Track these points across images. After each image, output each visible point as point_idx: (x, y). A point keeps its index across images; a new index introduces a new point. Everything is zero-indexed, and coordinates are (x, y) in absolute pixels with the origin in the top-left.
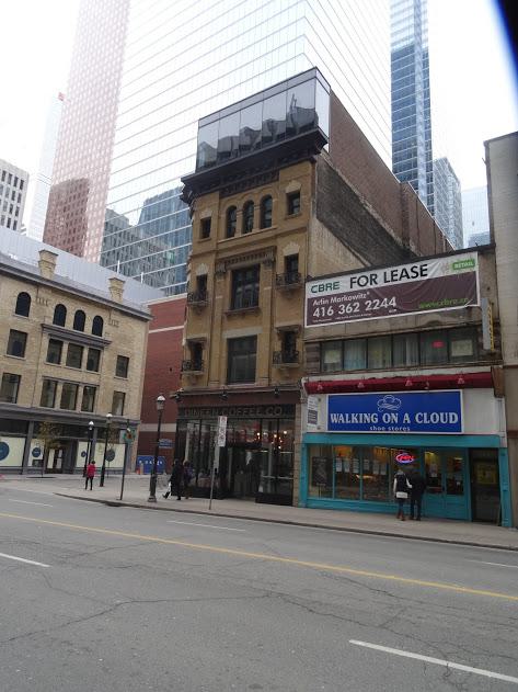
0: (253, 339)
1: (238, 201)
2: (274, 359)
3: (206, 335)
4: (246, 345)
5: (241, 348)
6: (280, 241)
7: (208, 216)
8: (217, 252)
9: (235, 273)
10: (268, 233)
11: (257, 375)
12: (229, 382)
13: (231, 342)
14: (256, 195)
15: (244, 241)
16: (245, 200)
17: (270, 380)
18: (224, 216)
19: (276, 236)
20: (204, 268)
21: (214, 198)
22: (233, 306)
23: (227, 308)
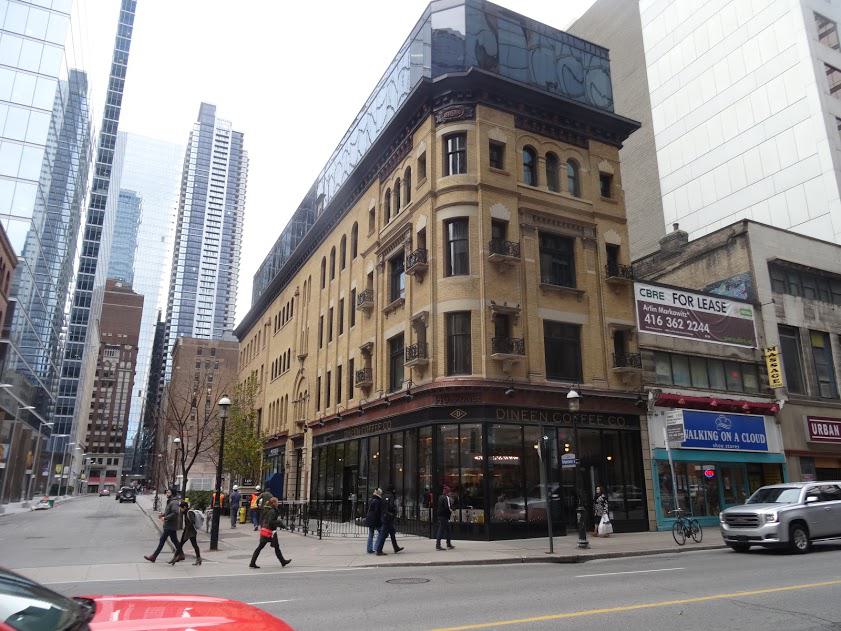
3: (373, 340)
15: (400, 219)
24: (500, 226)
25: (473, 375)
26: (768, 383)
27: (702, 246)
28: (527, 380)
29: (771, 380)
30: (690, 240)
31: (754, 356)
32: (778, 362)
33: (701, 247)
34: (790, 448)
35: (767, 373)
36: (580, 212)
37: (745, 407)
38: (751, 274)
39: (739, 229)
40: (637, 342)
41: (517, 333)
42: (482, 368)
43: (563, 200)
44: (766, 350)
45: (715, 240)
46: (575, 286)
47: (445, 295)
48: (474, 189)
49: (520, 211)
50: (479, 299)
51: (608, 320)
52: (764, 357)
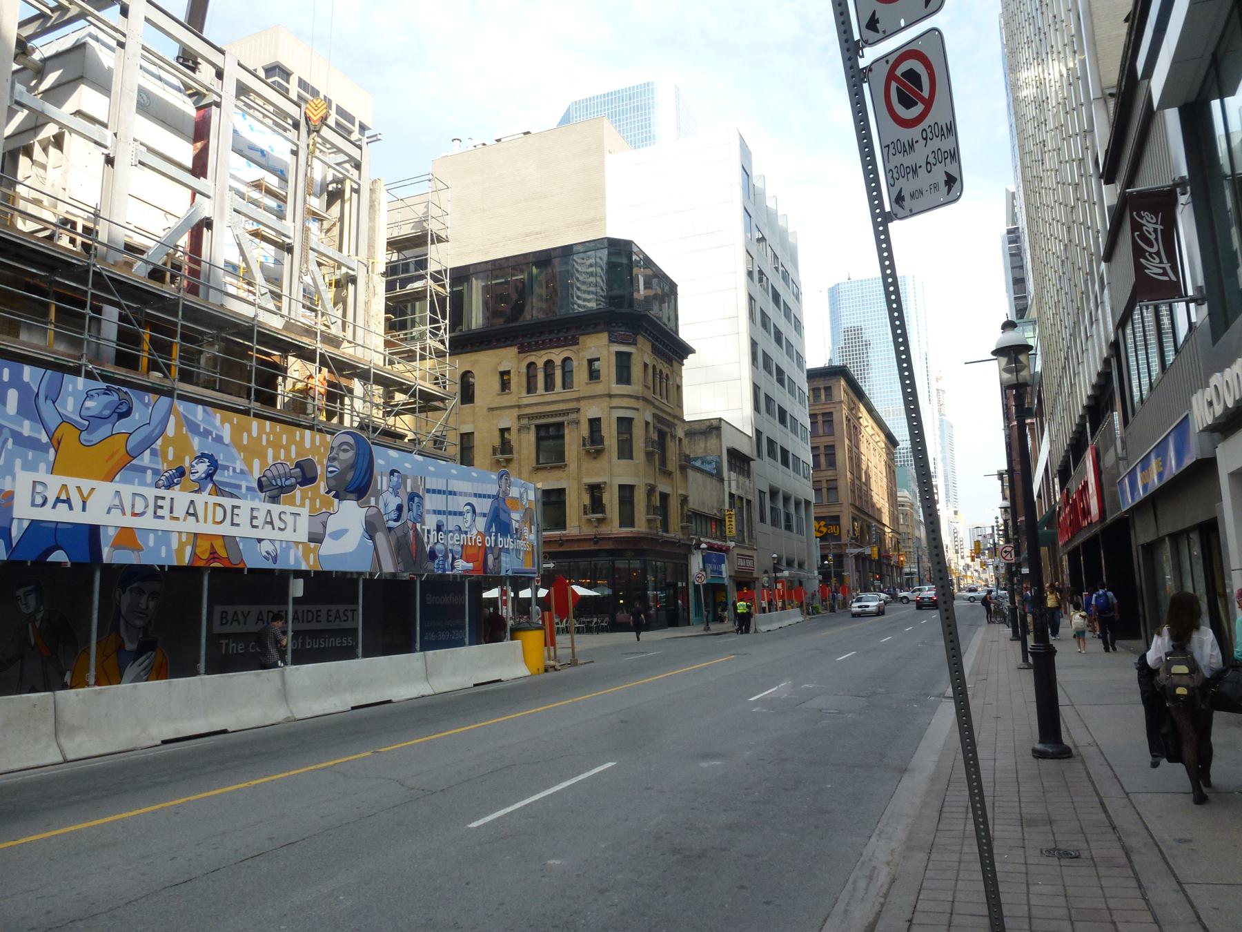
0: (561, 492)
1: (540, 358)
6: (582, 404)
8: (519, 407)
9: (538, 427)
14: (557, 356)
16: (545, 359)
18: (524, 370)
19: (578, 400)
20: (507, 420)
21: (512, 351)
24: (647, 423)
25: (635, 529)
36: (669, 414)
38: (720, 457)
39: (715, 423)
42: (641, 526)
45: (696, 426)
47: (616, 472)
48: (637, 398)
49: (655, 416)
51: (680, 492)
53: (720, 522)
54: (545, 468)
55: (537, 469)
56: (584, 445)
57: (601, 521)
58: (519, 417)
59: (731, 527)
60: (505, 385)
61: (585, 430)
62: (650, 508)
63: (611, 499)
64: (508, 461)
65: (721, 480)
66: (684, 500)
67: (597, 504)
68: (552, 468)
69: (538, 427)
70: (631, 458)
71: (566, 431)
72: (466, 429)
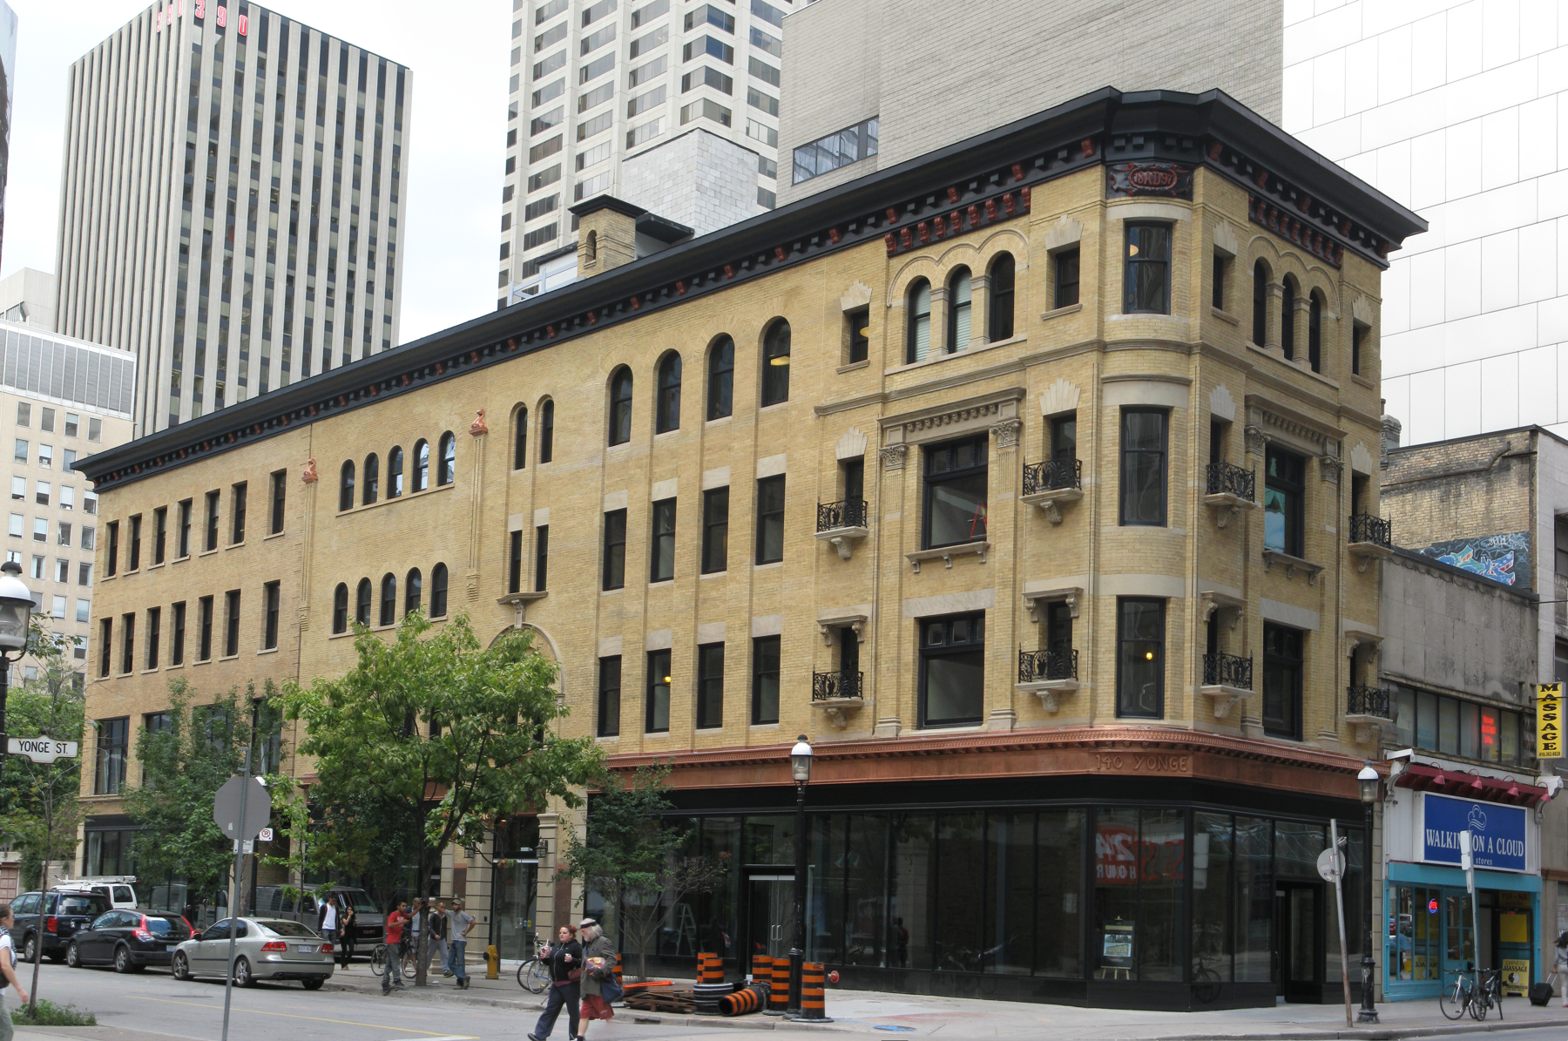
0: (975, 619)
2: (1026, 668)
3: (866, 610)
4: (959, 628)
5: (951, 645)
6: (1030, 379)
7: (860, 302)
8: (884, 398)
9: (929, 450)
10: (1005, 353)
11: (986, 710)
12: (923, 721)
13: (924, 623)
17: (1014, 721)
18: (899, 301)
19: (1022, 365)
20: (856, 439)
22: (926, 540)
23: (912, 546)
25: (1166, 722)
26: (1534, 750)
27: (1436, 460)
28: (1241, 734)
29: (1540, 743)
30: (1403, 443)
31: (1520, 697)
32: (1559, 712)
33: (1433, 464)
34: (1548, 866)
35: (1533, 730)
37: (1513, 791)
40: (1379, 666)
41: (1233, 646)
43: (1270, 365)
44: (1539, 688)
46: (1301, 556)
47: (1112, 561)
50: (1183, 575)
51: (1348, 624)
52: (1532, 699)
53: (1523, 718)
54: (938, 559)
55: (919, 562)
56: (1027, 489)
57: (1063, 698)
58: (885, 426)
59: (1551, 736)
60: (858, 350)
61: (1034, 448)
62: (1214, 665)
63: (1096, 640)
64: (856, 543)
65: (1526, 598)
66: (1364, 651)
67: (1057, 655)
68: (954, 557)
69: (929, 450)
70: (1162, 522)
71: (992, 454)
72: (767, 468)
